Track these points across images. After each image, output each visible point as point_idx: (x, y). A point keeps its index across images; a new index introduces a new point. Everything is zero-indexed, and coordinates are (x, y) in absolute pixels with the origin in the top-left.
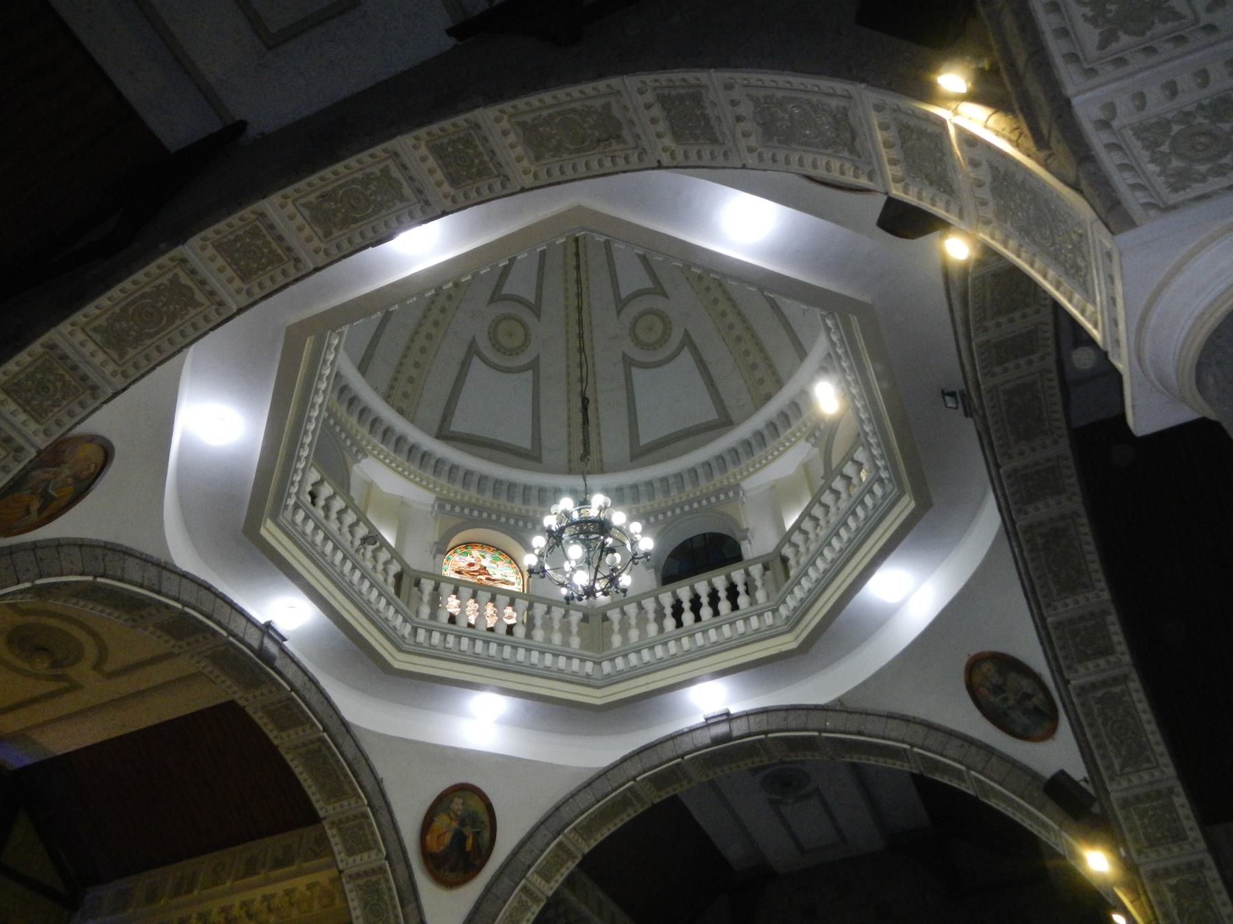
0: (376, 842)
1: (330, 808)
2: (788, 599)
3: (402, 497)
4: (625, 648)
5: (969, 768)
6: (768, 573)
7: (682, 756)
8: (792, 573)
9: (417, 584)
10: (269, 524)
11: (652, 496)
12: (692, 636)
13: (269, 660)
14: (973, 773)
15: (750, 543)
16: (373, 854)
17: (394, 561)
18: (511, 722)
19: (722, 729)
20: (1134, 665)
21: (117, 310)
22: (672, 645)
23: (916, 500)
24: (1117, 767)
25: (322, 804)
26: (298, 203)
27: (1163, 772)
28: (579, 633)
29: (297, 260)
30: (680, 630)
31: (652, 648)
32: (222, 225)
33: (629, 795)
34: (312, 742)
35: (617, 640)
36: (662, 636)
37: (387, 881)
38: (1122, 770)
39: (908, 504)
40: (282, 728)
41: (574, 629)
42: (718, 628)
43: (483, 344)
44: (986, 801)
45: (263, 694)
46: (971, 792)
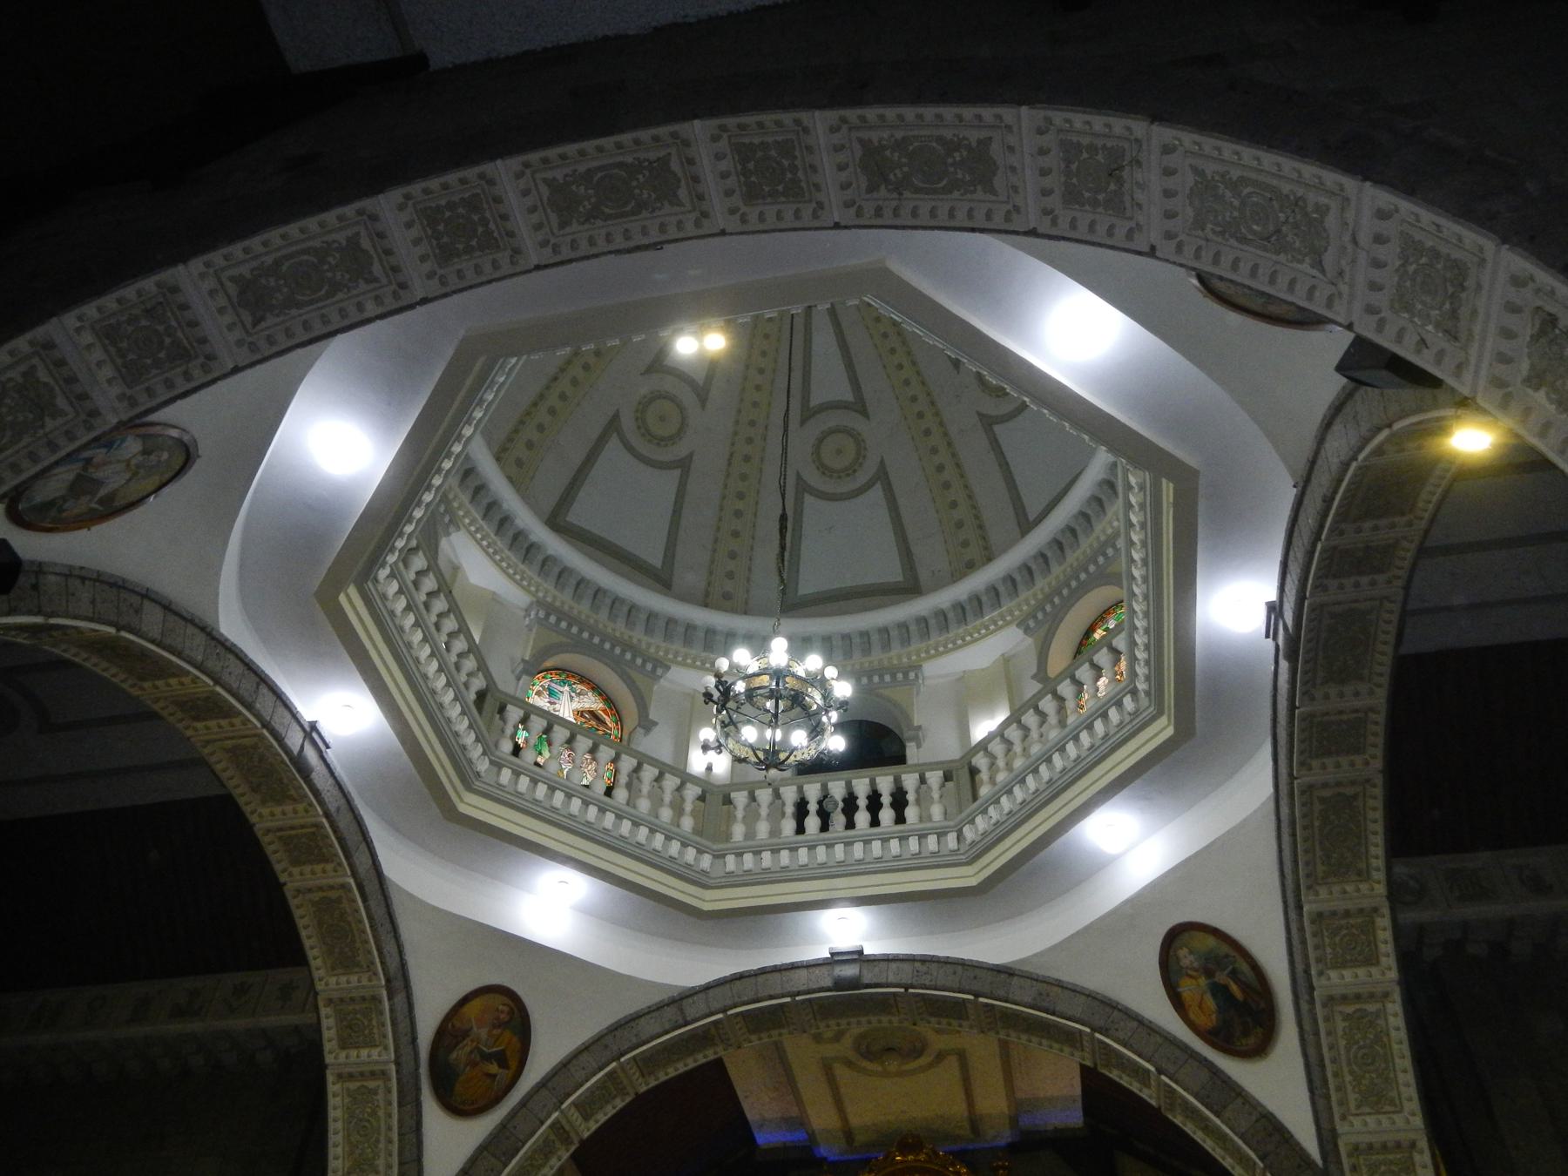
0: (385, 1036)
1: (333, 980)
2: (979, 820)
3: (494, 593)
4: (775, 840)
5: (1160, 1071)
6: (950, 785)
7: (793, 995)
8: (984, 791)
9: (502, 710)
10: (352, 591)
11: (867, 650)
12: (812, 848)
13: (304, 770)
14: (1163, 1077)
15: (919, 746)
16: (375, 1052)
17: (480, 674)
18: (586, 910)
19: (849, 971)
20: (1400, 983)
21: (269, 260)
22: (839, 849)
23: (1176, 728)
24: (1352, 1105)
25: (322, 972)
26: (538, 176)
27: (1408, 1122)
28: (694, 813)
29: (516, 251)
30: (800, 838)
31: (757, 853)
32: (434, 183)
33: (713, 1031)
34: (332, 888)
35: (738, 831)
36: (775, 840)
37: (389, 1091)
38: (1358, 1107)
39: (1164, 728)
40: (296, 862)
41: (688, 807)
42: (848, 844)
43: (627, 422)
44: (1170, 1117)
45: (284, 813)
46: (1153, 1103)
